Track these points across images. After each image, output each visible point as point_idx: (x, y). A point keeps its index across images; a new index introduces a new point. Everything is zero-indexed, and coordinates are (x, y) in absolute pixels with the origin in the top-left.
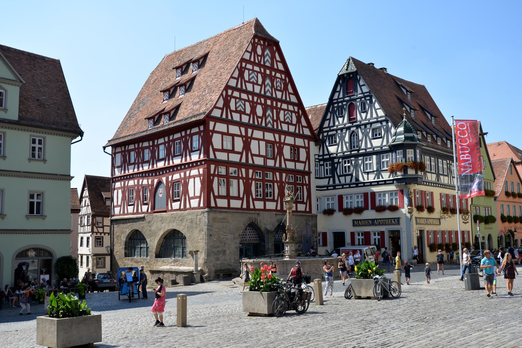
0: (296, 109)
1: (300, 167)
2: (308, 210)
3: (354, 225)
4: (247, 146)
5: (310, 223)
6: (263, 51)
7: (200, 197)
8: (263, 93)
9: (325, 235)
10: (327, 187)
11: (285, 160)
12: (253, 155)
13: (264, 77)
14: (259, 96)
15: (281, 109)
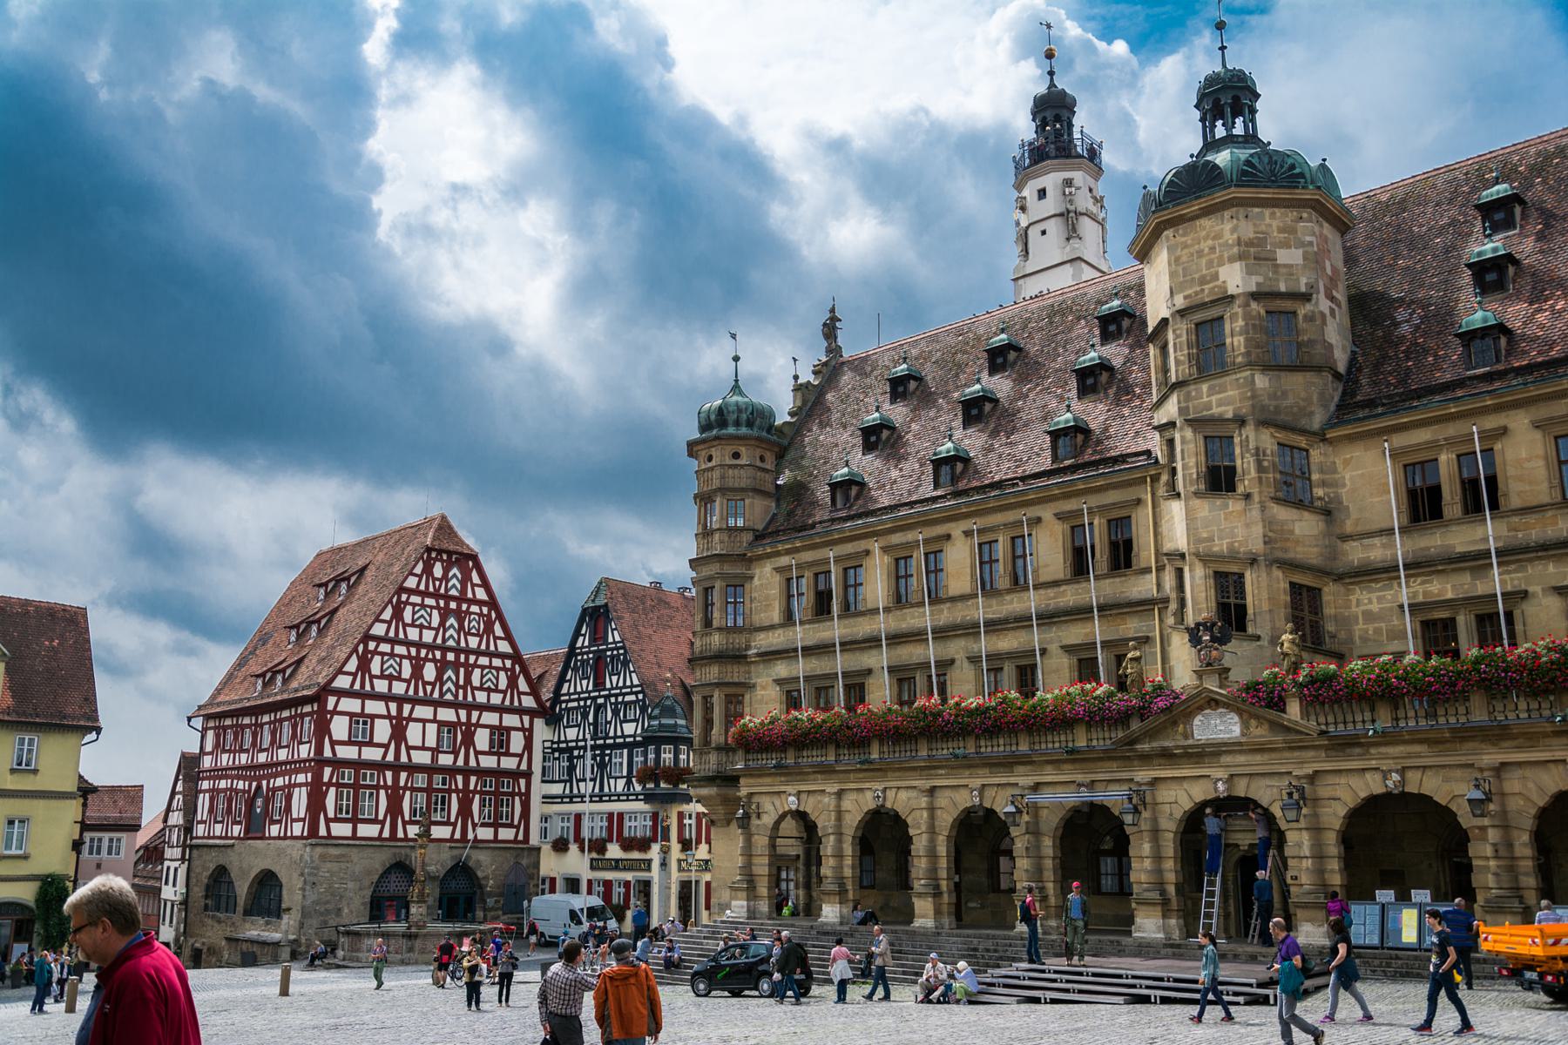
0: (508, 663)
1: (509, 763)
2: (520, 837)
3: (592, 868)
4: (399, 734)
5: (524, 862)
6: (446, 571)
7: (303, 820)
8: (439, 641)
9: (553, 880)
10: (561, 799)
11: (477, 753)
12: (409, 748)
13: (445, 614)
14: (431, 647)
15: (475, 665)
